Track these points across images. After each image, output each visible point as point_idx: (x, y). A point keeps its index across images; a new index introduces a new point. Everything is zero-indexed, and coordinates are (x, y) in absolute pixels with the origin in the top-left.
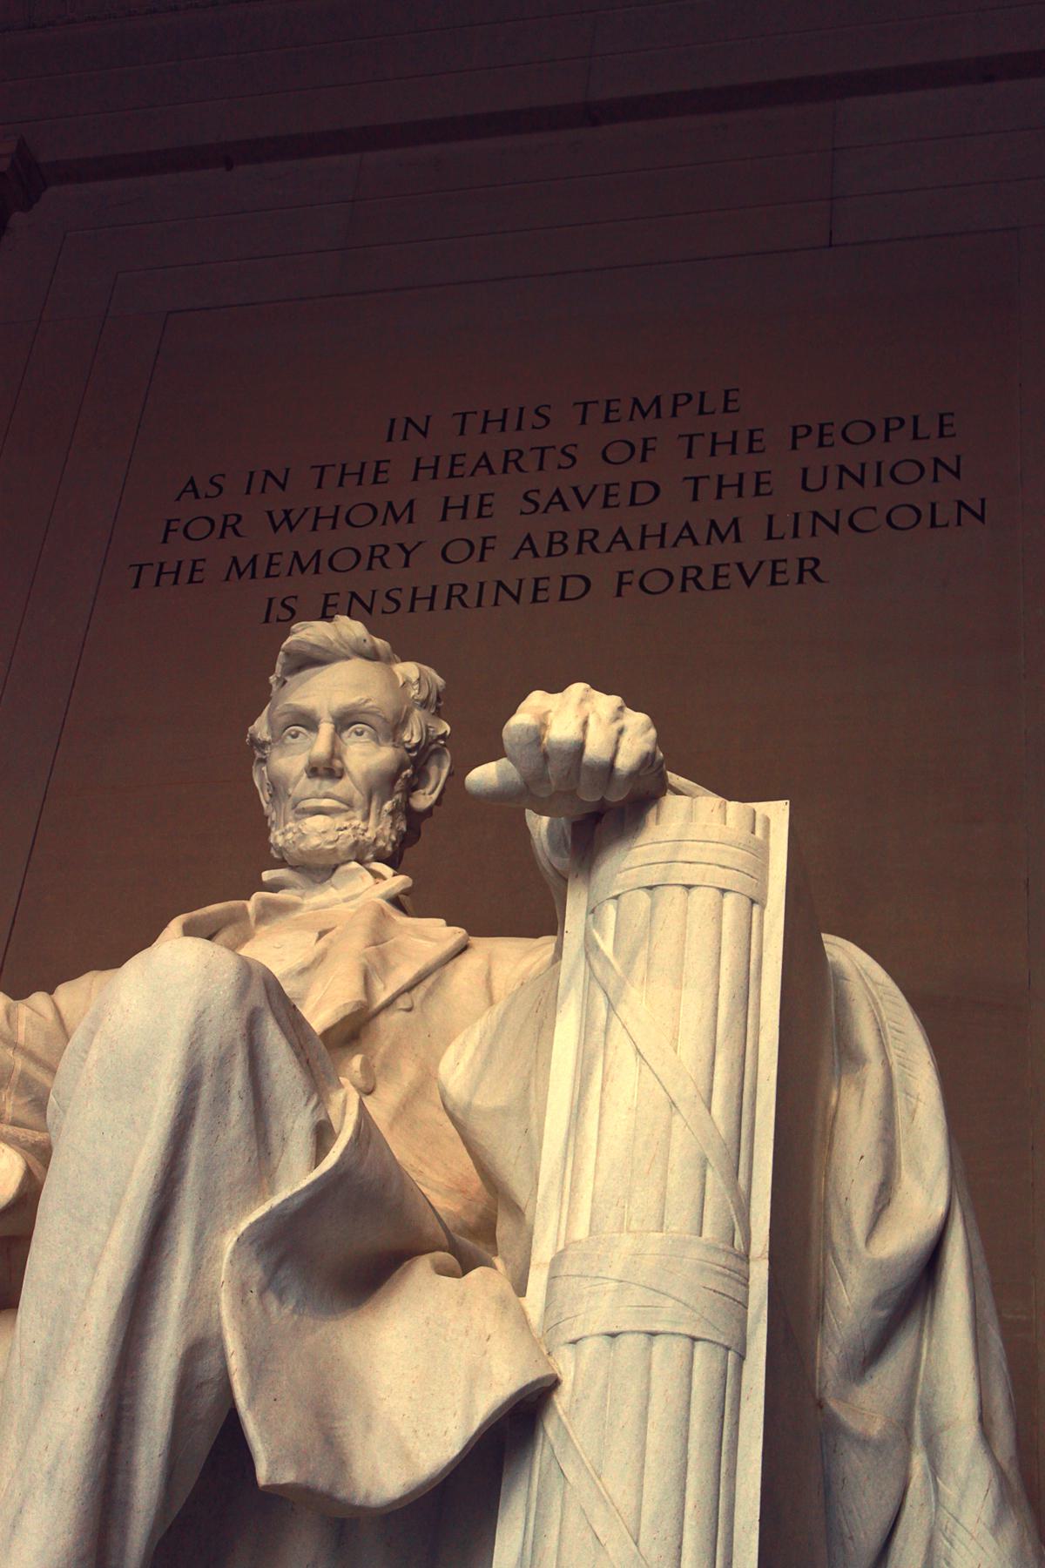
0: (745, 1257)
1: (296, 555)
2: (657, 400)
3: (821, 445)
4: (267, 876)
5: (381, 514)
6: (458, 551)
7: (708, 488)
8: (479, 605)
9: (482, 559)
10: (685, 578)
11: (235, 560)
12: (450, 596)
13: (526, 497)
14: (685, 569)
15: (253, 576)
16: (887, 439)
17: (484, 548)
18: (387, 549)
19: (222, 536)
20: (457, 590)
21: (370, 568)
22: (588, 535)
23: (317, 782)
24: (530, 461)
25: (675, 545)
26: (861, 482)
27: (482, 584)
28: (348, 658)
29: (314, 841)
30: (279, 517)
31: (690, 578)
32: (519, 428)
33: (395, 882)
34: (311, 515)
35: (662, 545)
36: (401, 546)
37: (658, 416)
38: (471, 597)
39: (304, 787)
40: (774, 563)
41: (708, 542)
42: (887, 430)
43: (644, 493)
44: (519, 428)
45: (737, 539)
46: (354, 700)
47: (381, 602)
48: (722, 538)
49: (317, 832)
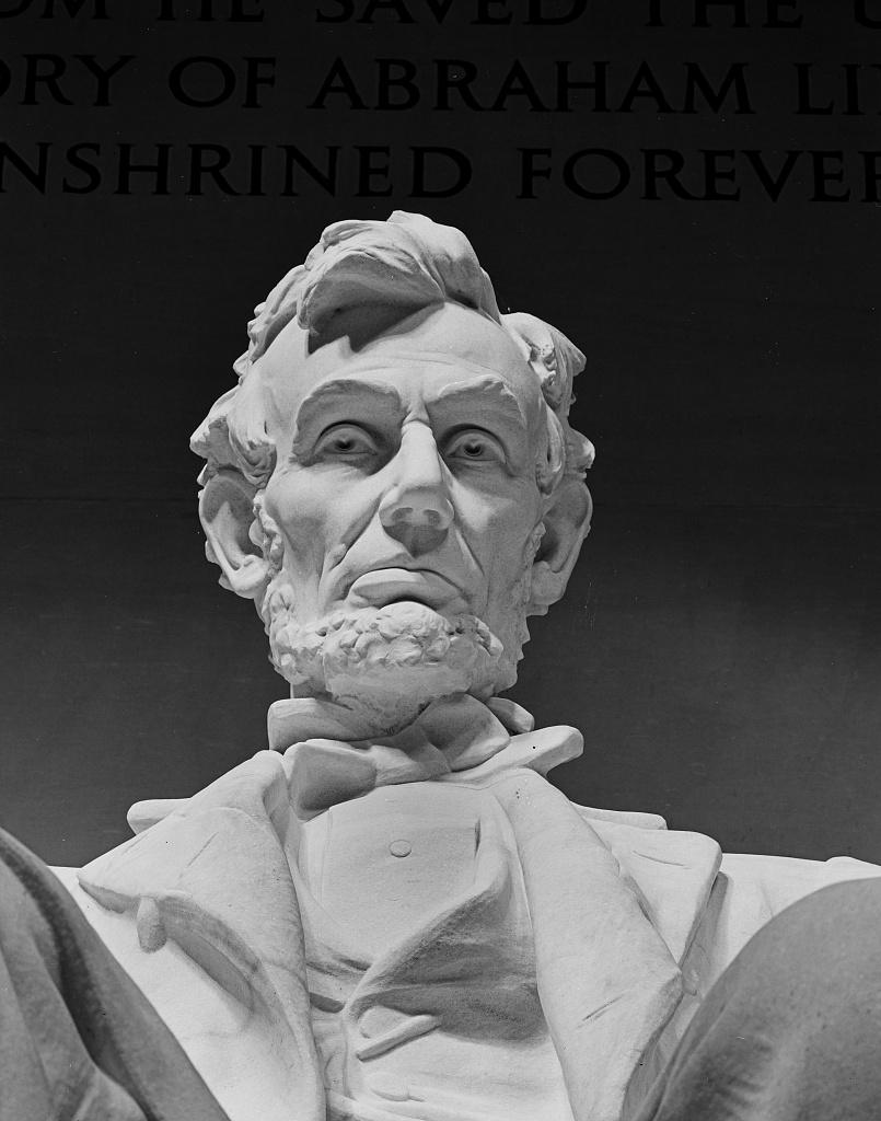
8: (256, 189)
9: (251, 102)
10: (651, 175)
12: (197, 169)
14: (650, 155)
18: (60, 66)
20: (209, 159)
25: (626, 108)
27: (257, 151)
29: (407, 651)
35: (600, 105)
36: (88, 60)
39: (376, 543)
40: (818, 157)
41: (689, 109)
45: (744, 108)
46: (476, 380)
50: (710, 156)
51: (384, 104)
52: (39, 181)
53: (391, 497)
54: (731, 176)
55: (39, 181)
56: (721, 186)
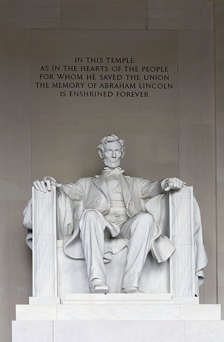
0: (191, 236)
2: (120, 59)
3: (147, 71)
4: (105, 168)
5: (77, 78)
6: (91, 86)
7: (130, 77)
8: (95, 96)
12: (91, 94)
13: (100, 76)
14: (127, 92)
15: (57, 87)
16: (157, 71)
17: (95, 85)
19: (50, 79)
20: (92, 93)
21: (76, 87)
22: (111, 85)
23: (112, 158)
24: (100, 69)
25: (125, 88)
27: (95, 92)
28: (115, 141)
31: (128, 94)
32: (98, 62)
33: (123, 171)
34: (65, 75)
35: (123, 88)
36: (81, 83)
37: (121, 62)
38: (94, 94)
41: (131, 88)
42: (157, 69)
43: (120, 77)
44: (98, 62)
45: (135, 88)
47: (79, 94)
48: (133, 87)
49: (113, 165)
50: (132, 92)
51: (106, 88)
52: (78, 95)
53: (112, 157)
54: (134, 94)
55: (78, 95)
56: (133, 95)
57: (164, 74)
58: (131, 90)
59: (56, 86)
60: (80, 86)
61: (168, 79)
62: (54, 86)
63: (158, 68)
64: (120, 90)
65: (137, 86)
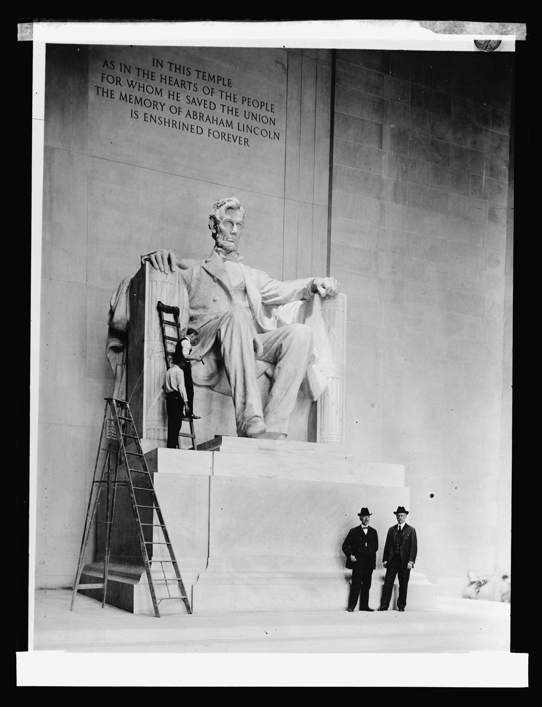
1: (136, 98)
2: (214, 76)
7: (226, 109)
11: (121, 94)
15: (126, 101)
19: (117, 84)
20: (174, 123)
22: (201, 115)
26: (256, 119)
30: (130, 83)
31: (223, 135)
32: (184, 74)
34: (138, 84)
37: (214, 82)
38: (177, 125)
42: (261, 106)
43: (213, 107)
44: (184, 74)
47: (157, 120)
52: (155, 122)
55: (155, 122)
57: (269, 115)
58: (227, 130)
59: (125, 99)
60: (159, 106)
61: (274, 124)
62: (122, 99)
63: (263, 104)
64: (214, 127)
65: (235, 126)
